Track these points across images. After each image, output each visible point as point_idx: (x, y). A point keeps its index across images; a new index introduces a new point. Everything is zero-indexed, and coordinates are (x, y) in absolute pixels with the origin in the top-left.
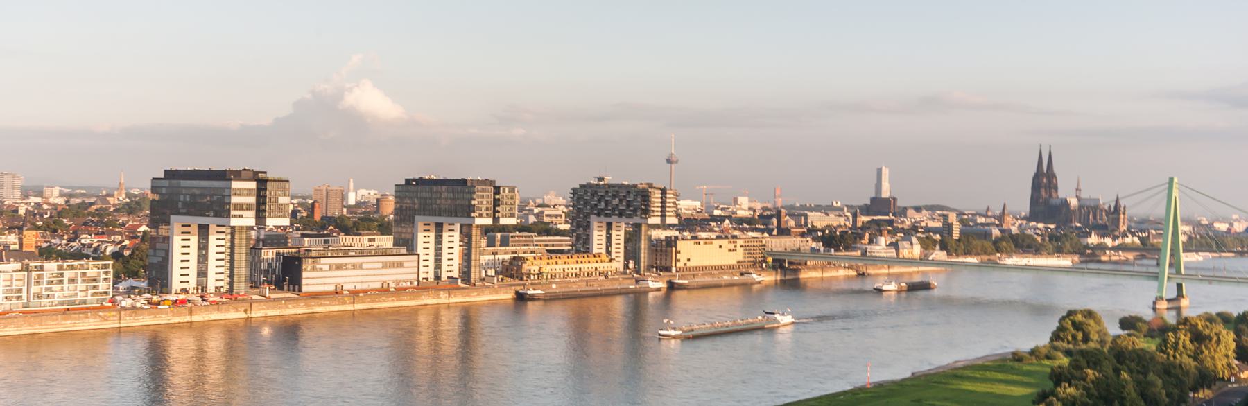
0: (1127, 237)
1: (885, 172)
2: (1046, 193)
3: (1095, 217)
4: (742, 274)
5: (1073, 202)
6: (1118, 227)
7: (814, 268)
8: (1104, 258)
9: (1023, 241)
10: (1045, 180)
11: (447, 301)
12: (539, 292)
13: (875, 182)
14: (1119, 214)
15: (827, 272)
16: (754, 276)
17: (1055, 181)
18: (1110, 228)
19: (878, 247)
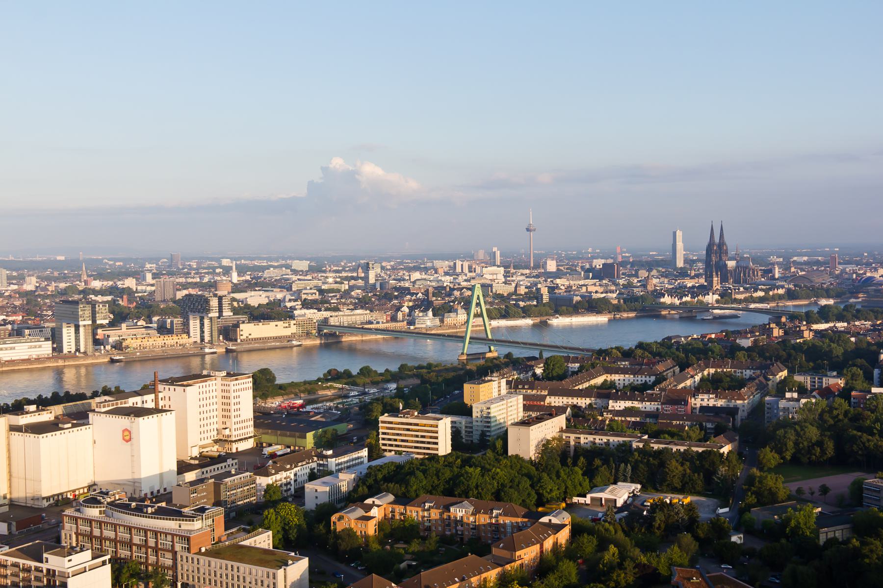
0: (709, 295)
1: (679, 234)
2: (717, 257)
3: (745, 275)
4: (288, 341)
5: (731, 264)
6: (712, 287)
7: (356, 335)
8: (663, 313)
9: (596, 304)
10: (715, 248)
11: (63, 364)
12: (122, 357)
13: (672, 243)
14: (713, 278)
15: (365, 336)
16: (294, 342)
17: (725, 248)
18: (708, 288)
19: (427, 318)
